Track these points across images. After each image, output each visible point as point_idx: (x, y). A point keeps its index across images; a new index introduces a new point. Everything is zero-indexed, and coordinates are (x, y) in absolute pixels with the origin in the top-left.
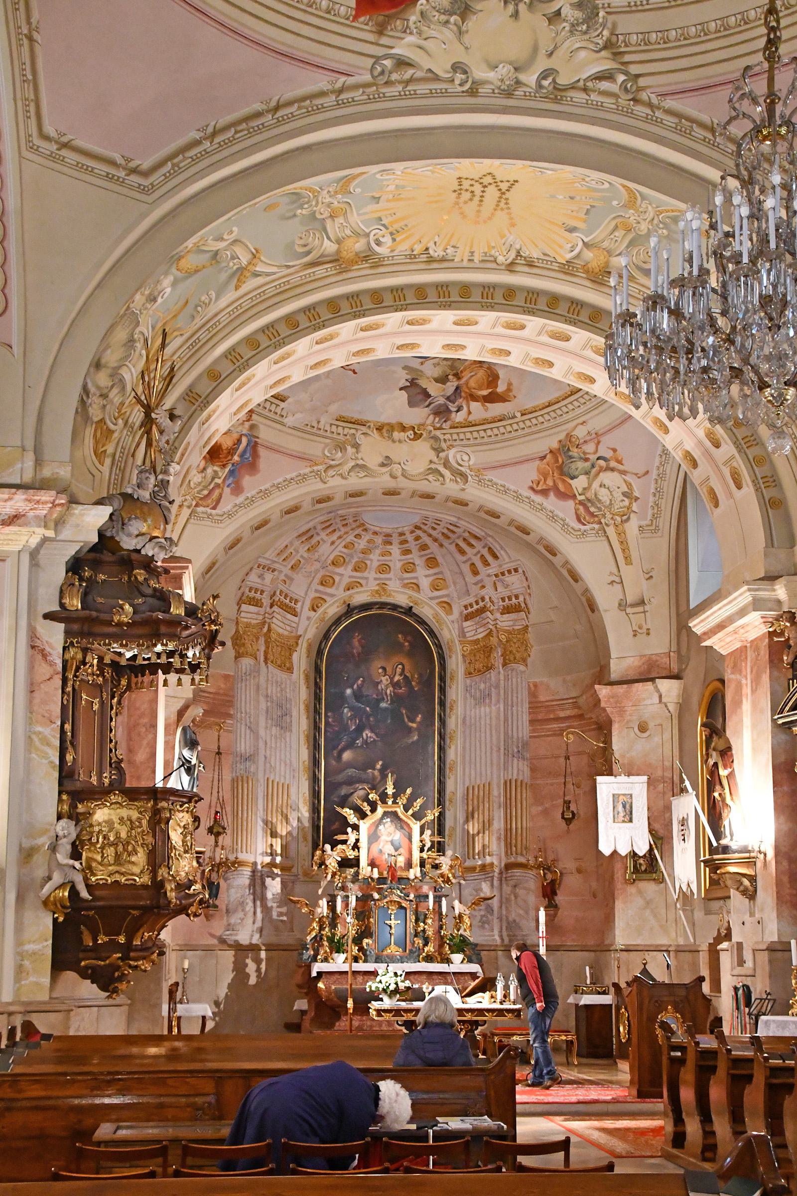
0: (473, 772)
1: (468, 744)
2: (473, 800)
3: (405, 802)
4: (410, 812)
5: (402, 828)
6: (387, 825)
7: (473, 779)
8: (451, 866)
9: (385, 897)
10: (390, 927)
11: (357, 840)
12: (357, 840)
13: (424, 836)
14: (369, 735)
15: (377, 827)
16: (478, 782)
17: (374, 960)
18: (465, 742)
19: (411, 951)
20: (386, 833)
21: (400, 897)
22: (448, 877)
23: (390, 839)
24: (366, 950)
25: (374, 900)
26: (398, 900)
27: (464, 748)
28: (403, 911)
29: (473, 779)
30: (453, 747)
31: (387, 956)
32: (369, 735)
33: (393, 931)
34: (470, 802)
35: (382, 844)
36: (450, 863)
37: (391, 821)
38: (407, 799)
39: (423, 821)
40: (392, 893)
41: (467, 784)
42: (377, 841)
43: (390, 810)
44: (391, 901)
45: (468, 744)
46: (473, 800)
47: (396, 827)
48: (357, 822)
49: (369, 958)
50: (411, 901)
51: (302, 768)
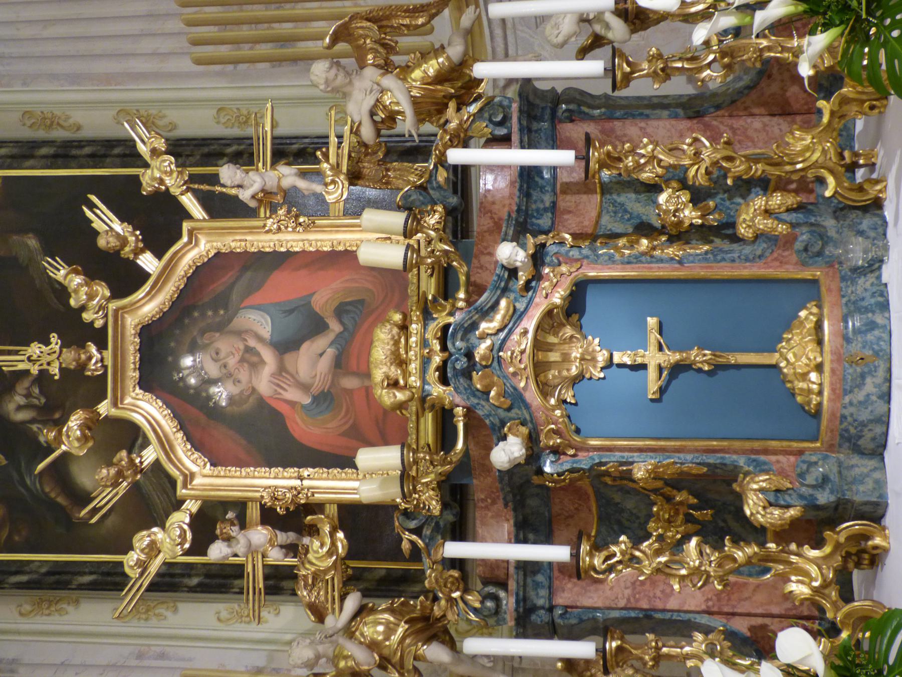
0: (147, 45)
1: (60, 67)
2: (236, 42)
3: (103, 290)
4: (148, 262)
5: (222, 301)
6: (213, 370)
7: (165, 45)
8: (386, 67)
9: (517, 399)
10: (677, 369)
11: (269, 517)
12: (269, 517)
13: (245, 195)
14: (20, 400)
15: (214, 412)
16: (176, 25)
17: (862, 465)
18: (53, 77)
19: (810, 255)
20: (243, 375)
21: (516, 316)
22: (441, 78)
23: (268, 356)
24: (812, 506)
25: (534, 455)
26: (530, 323)
27: (75, 79)
28: (593, 300)
29: (165, 45)
30: (78, 116)
31: (842, 389)
32: (20, 400)
33: (700, 357)
34: (246, 51)
35: (293, 394)
36: (371, 73)
37: (193, 349)
38: (91, 275)
39: (189, 202)
40: (495, 359)
41: (186, 65)
42: (276, 418)
43: (132, 358)
44: (540, 367)
45: (60, 67)
46: (236, 42)
47: (221, 327)
48: (180, 519)
49: (860, 494)
50: (538, 258)
51: (135, 626)
